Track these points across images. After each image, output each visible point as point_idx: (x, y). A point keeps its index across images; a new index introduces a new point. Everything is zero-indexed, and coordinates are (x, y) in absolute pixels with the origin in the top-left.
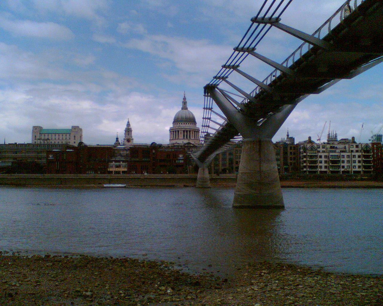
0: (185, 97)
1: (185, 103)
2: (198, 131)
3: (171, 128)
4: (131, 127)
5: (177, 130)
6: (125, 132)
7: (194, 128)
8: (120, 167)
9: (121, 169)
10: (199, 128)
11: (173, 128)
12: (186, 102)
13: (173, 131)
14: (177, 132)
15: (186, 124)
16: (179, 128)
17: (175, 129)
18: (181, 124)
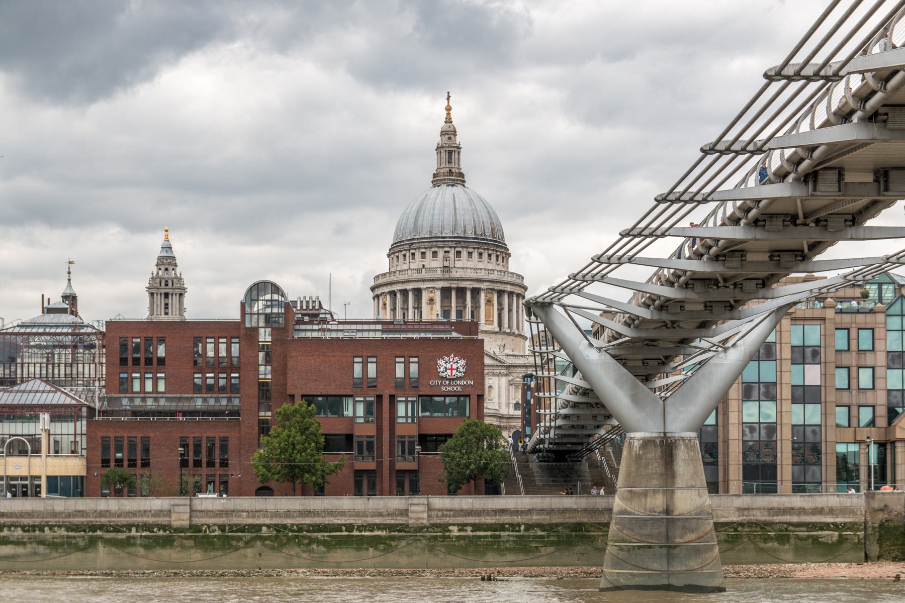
0: (449, 120)
1: (450, 153)
2: (518, 290)
3: (384, 275)
4: (178, 270)
5: (409, 286)
6: (152, 294)
7: (495, 276)
8: (37, 451)
9: (44, 466)
10: (523, 278)
11: (394, 278)
12: (459, 148)
13: (393, 294)
14: (410, 295)
15: (459, 254)
16: (424, 275)
17: (404, 282)
18: (429, 254)
